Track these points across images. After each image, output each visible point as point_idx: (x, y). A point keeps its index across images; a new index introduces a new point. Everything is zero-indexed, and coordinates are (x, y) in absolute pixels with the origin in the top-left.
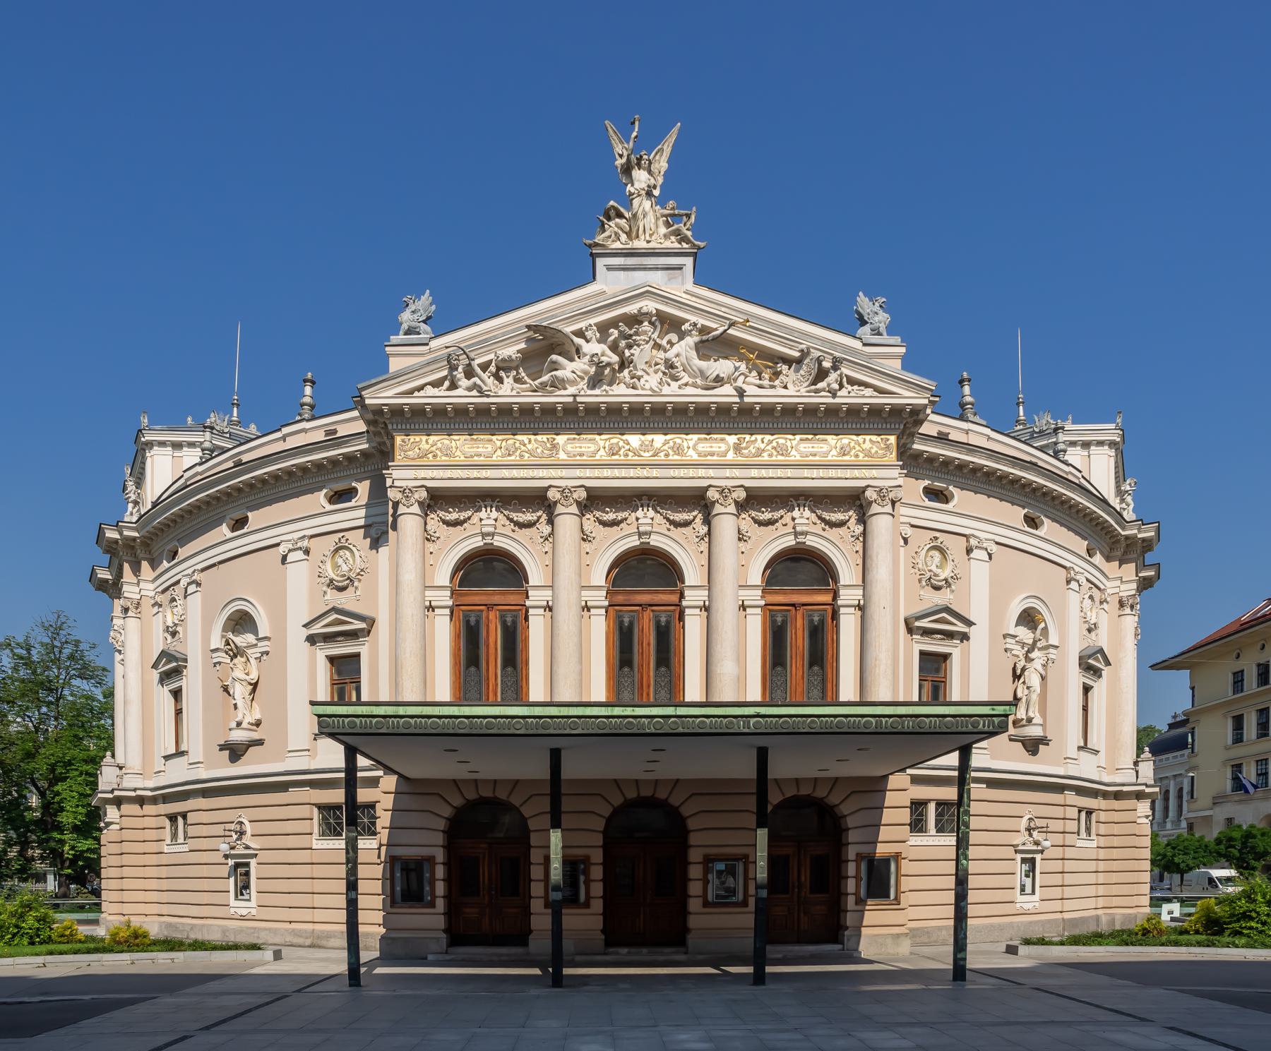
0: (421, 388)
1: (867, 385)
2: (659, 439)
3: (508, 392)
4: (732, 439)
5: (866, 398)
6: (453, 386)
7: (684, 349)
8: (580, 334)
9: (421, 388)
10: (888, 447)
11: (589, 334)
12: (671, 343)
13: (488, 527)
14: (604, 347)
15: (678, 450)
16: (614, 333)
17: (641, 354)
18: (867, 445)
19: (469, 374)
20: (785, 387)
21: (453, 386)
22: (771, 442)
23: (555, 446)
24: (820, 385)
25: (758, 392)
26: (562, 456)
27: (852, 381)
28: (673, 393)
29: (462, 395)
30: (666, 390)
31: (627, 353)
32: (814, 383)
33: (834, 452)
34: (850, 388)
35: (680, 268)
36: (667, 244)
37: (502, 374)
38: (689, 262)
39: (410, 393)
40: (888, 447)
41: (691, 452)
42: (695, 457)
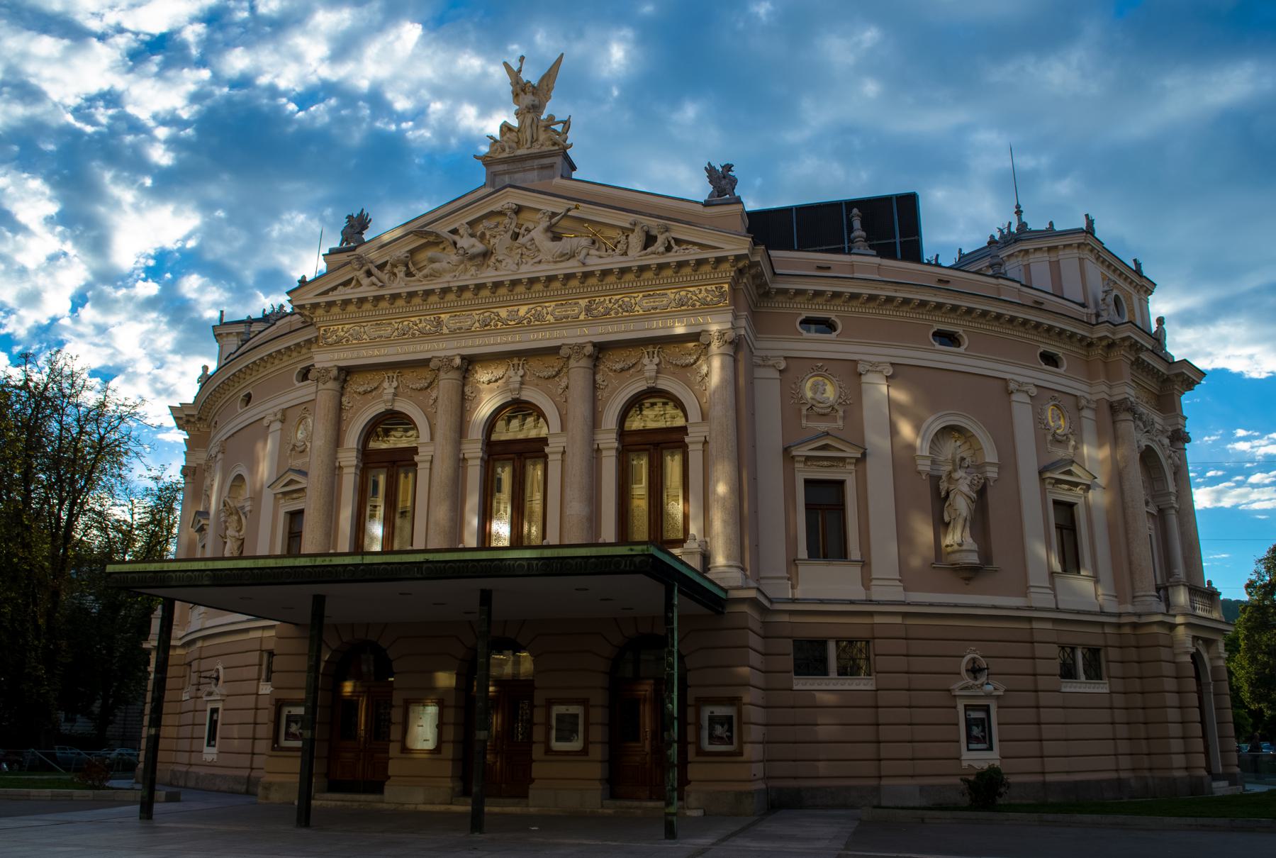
0: (334, 288)
1: (694, 244)
2: (523, 310)
3: (400, 285)
4: (583, 303)
5: (693, 254)
6: (359, 284)
7: (538, 234)
8: (455, 232)
9: (334, 288)
10: (722, 294)
11: (461, 231)
12: (528, 231)
13: (387, 395)
14: (473, 240)
15: (539, 317)
16: (480, 229)
17: (501, 242)
18: (704, 294)
19: (369, 274)
20: (625, 254)
21: (359, 284)
22: (617, 301)
23: (439, 323)
24: (649, 250)
25: (597, 262)
26: (445, 331)
27: (678, 242)
28: (527, 271)
29: (366, 289)
30: (524, 268)
31: (492, 241)
32: (645, 248)
33: (673, 304)
34: (676, 248)
35: (552, 166)
36: (545, 148)
37: (396, 270)
38: (559, 160)
39: (326, 293)
40: (722, 294)
41: (549, 317)
42: (552, 320)
